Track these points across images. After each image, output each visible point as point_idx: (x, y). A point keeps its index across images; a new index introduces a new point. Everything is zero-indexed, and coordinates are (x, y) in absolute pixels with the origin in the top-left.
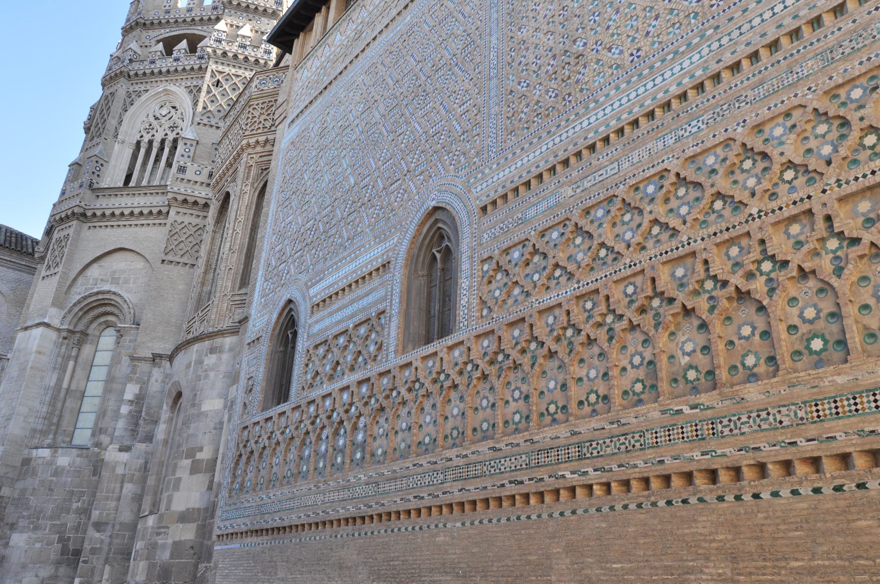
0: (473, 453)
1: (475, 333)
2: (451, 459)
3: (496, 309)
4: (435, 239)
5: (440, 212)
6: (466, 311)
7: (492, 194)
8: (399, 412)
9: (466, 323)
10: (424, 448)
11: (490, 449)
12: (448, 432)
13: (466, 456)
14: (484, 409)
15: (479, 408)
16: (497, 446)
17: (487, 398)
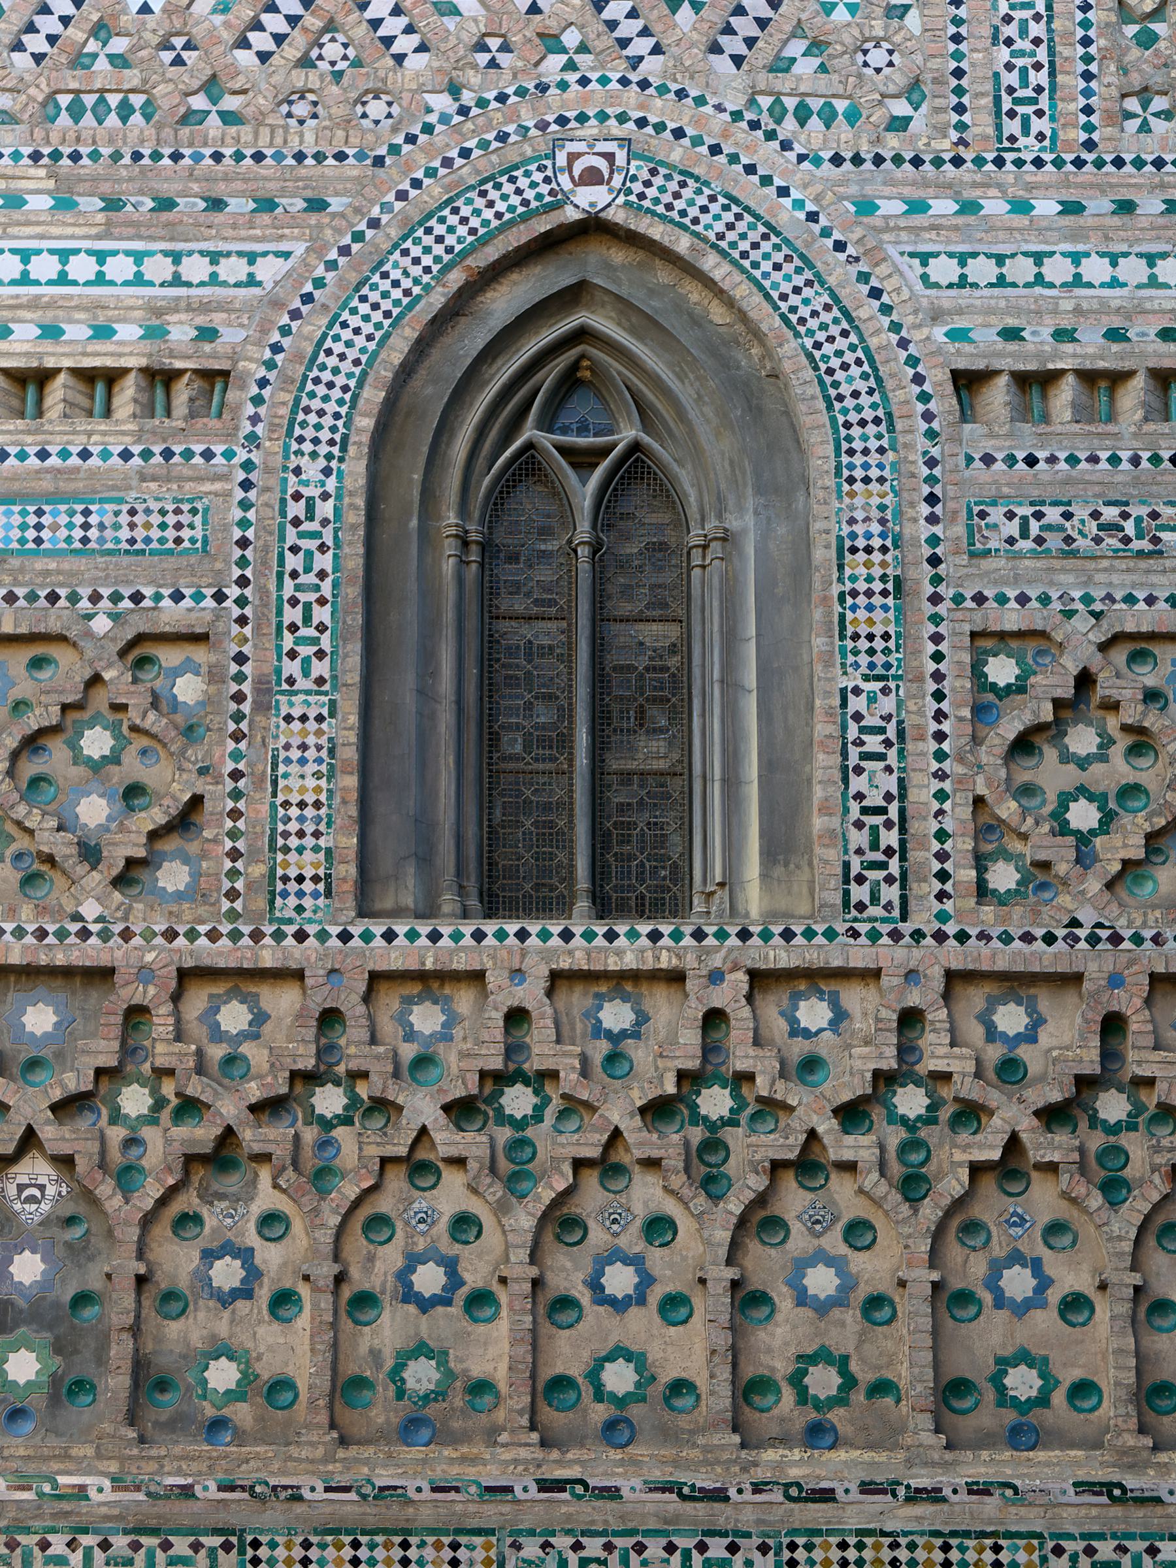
0: (979, 1490)
1: (954, 956)
2: (826, 1496)
3: (1094, 885)
4: (549, 375)
5: (618, 256)
6: (890, 838)
7: (1039, 336)
8: (384, 1204)
9: (891, 893)
10: (600, 1413)
11: (1083, 1487)
12: (781, 1367)
13: (933, 1495)
14: (1022, 1309)
15: (987, 1297)
16: (1130, 1482)
17: (1036, 1266)
